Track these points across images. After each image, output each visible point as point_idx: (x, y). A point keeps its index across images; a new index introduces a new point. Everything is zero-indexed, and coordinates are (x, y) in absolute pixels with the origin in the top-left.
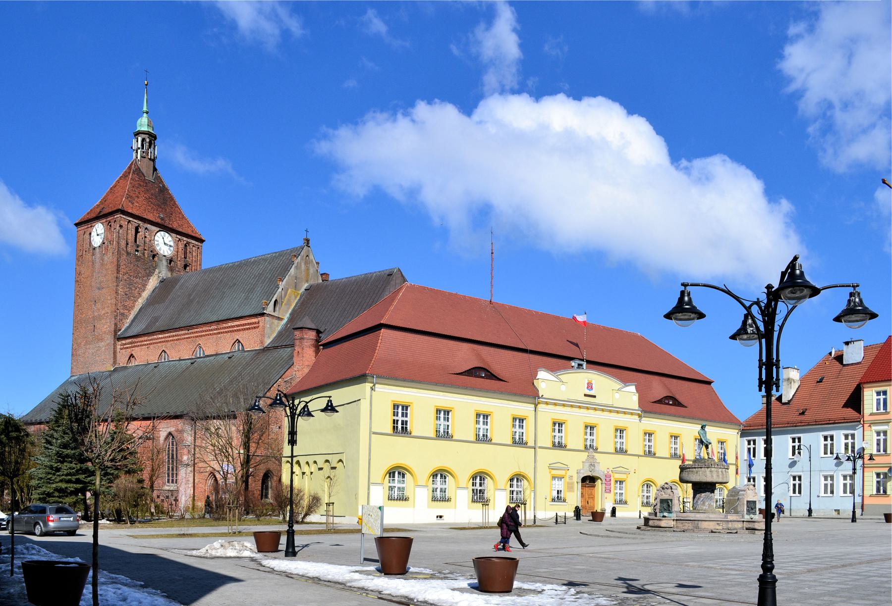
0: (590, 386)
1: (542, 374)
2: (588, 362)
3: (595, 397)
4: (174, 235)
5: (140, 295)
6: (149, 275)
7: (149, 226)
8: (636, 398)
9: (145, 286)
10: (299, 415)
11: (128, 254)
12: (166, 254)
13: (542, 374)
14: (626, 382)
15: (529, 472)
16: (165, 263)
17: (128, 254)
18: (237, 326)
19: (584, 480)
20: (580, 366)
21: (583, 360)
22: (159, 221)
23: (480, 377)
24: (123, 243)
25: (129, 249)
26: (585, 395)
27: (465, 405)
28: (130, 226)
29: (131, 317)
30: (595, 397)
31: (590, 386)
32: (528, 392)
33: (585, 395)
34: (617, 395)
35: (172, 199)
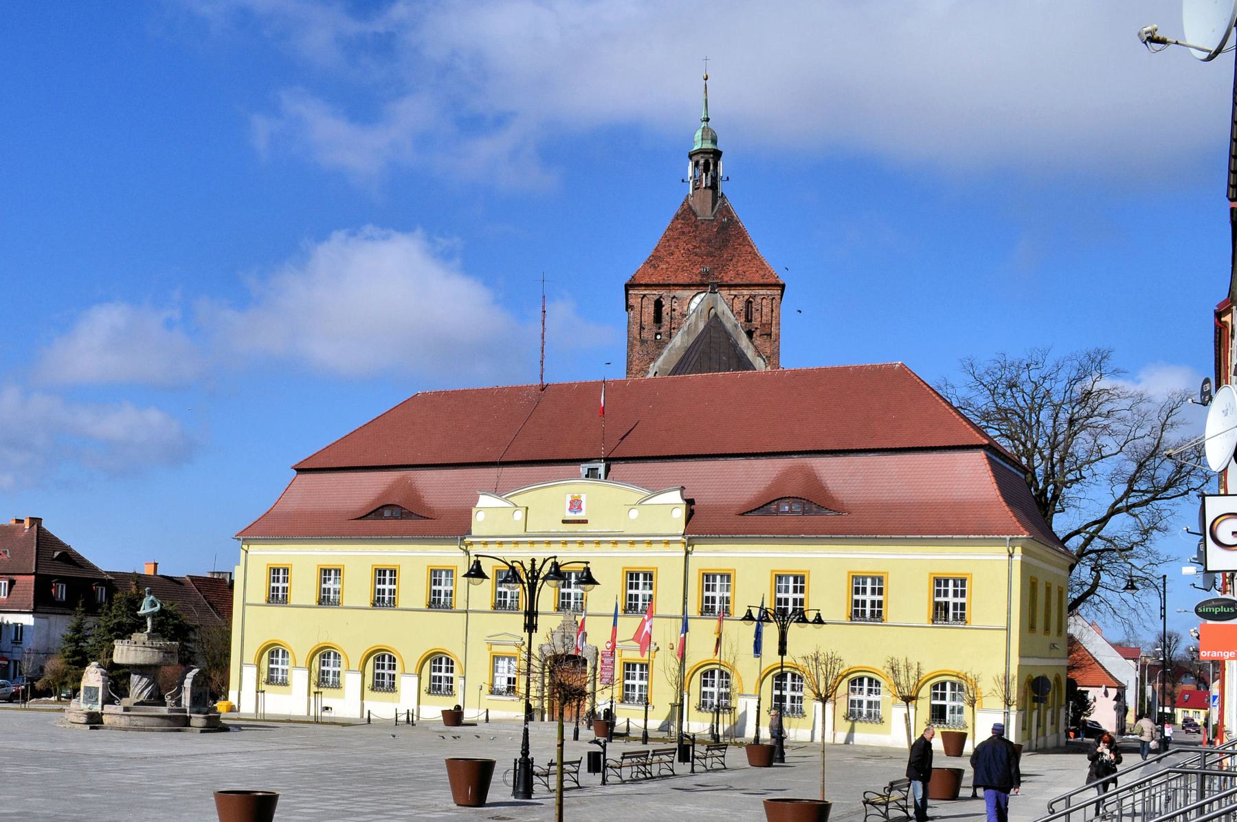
0: (576, 505)
1: (485, 501)
3: (585, 522)
7: (679, 293)
8: (680, 513)
10: (545, 578)
11: (643, 342)
13: (485, 501)
14: (657, 489)
15: (456, 653)
17: (643, 342)
22: (698, 279)
24: (636, 329)
25: (645, 335)
26: (564, 522)
27: (358, 559)
28: (645, 301)
30: (585, 522)
31: (576, 505)
32: (455, 527)
33: (564, 522)
34: (634, 514)
35: (741, 234)
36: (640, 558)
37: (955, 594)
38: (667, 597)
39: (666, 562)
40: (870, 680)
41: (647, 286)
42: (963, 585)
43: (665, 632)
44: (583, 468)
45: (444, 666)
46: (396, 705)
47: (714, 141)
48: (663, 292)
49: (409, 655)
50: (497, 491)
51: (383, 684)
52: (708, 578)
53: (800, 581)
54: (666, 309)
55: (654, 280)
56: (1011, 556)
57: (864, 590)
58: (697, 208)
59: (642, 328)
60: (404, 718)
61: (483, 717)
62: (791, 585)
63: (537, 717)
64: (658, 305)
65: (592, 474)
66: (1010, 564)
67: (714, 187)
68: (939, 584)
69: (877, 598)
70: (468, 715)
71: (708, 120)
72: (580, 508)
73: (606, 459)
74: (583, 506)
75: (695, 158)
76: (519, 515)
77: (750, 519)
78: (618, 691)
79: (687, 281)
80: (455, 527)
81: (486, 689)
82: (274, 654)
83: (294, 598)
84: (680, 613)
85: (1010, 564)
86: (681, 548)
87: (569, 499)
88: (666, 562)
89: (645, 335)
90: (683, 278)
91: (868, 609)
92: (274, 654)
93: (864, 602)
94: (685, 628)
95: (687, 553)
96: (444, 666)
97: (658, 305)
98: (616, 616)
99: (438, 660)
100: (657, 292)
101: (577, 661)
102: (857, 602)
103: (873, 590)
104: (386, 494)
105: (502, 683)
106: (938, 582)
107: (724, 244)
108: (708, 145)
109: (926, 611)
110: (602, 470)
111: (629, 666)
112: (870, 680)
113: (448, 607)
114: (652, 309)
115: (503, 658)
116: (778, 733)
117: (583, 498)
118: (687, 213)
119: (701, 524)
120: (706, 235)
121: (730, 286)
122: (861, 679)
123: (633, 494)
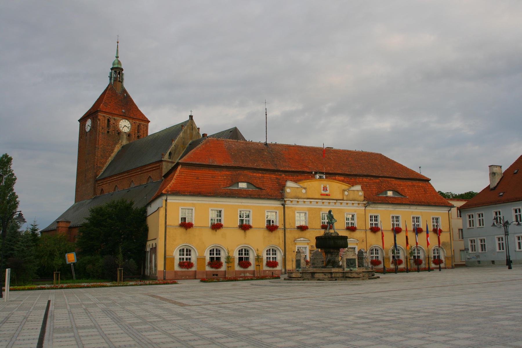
0: (325, 189)
1: (289, 184)
2: (327, 174)
3: (329, 195)
4: (131, 121)
5: (110, 156)
6: (116, 143)
7: (116, 118)
9: (113, 150)
12: (126, 131)
13: (289, 184)
16: (125, 136)
18: (150, 168)
20: (320, 177)
21: (323, 173)
26: (322, 195)
29: (104, 168)
30: (329, 195)
31: (325, 189)
50: (296, 181)
64: (109, 121)
72: (327, 190)
74: (328, 189)
87: (322, 186)
90: (117, 112)
97: (109, 121)
100: (107, 116)
110: (324, 177)
114: (106, 121)
117: (328, 186)
121: (133, 119)
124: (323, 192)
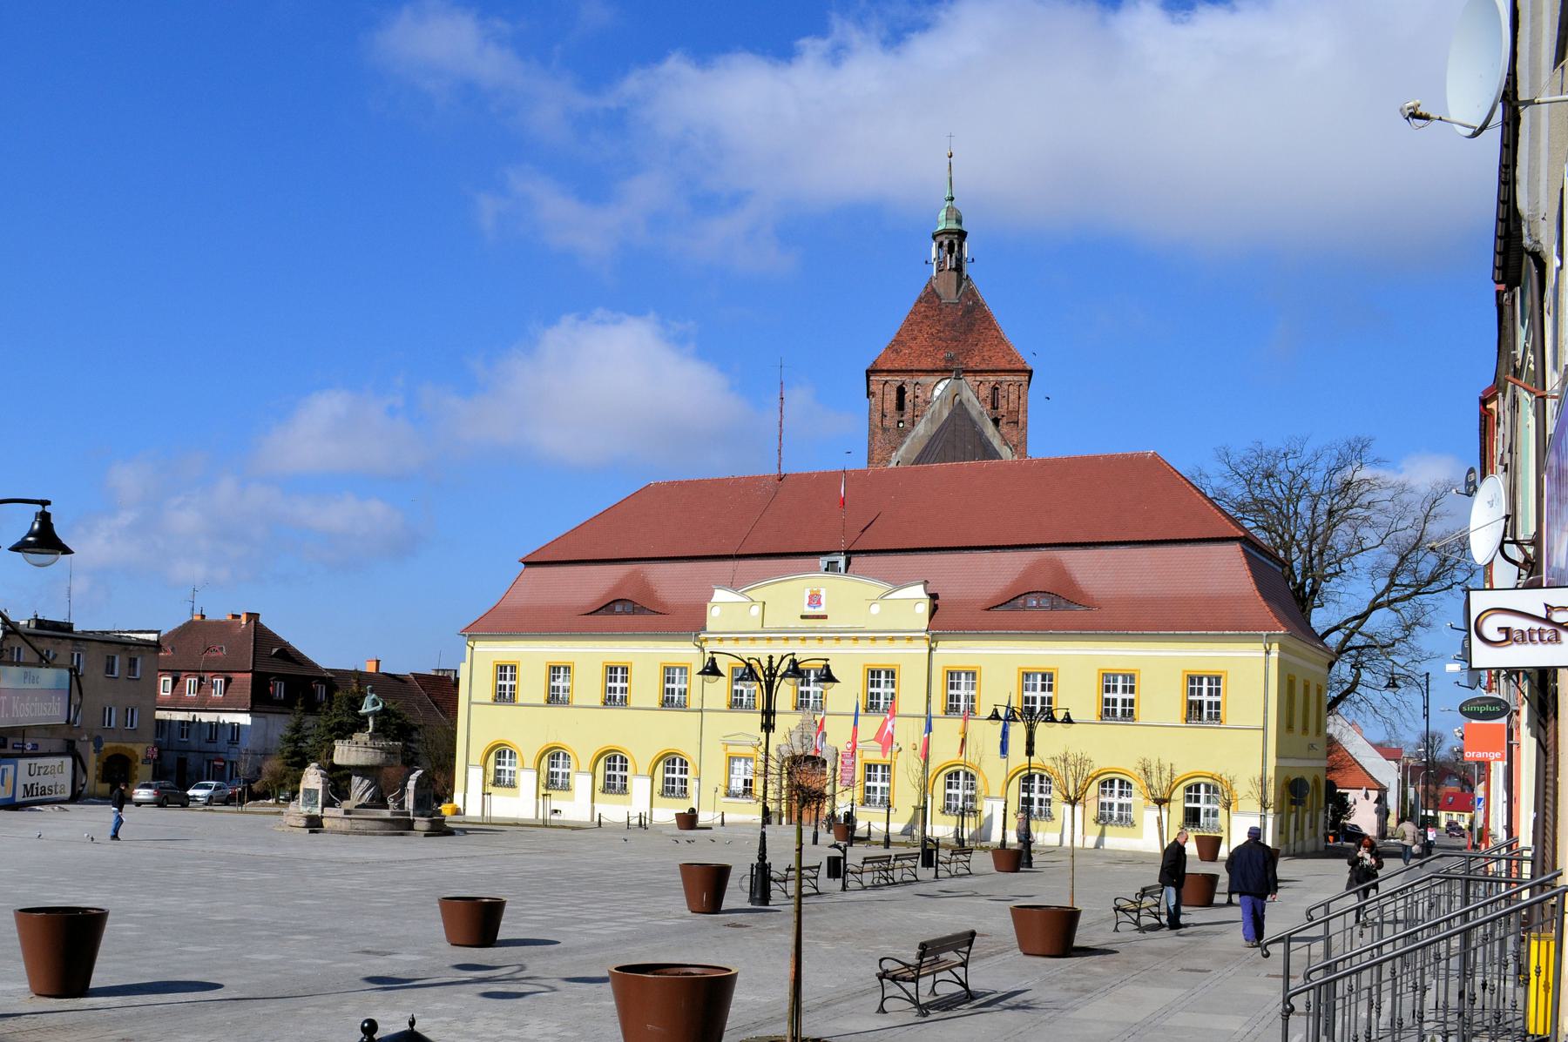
0: (815, 599)
1: (721, 595)
3: (825, 617)
7: (922, 379)
8: (923, 608)
10: (783, 676)
11: (885, 430)
13: (721, 595)
14: (899, 583)
15: (689, 752)
17: (885, 430)
19: (795, 760)
22: (941, 365)
23: (626, 612)
24: (877, 417)
27: (589, 657)
30: (825, 617)
31: (815, 599)
32: (690, 623)
34: (875, 609)
35: (987, 318)
36: (882, 654)
37: (1210, 692)
38: (910, 695)
39: (909, 658)
40: (1122, 782)
41: (889, 371)
42: (1218, 683)
43: (907, 732)
44: (823, 561)
45: (677, 767)
46: (628, 808)
47: (959, 221)
48: (906, 378)
49: (641, 757)
50: (733, 585)
51: (614, 785)
52: (953, 676)
53: (1048, 679)
54: (908, 396)
55: (897, 366)
56: (1268, 652)
57: (1115, 688)
58: (941, 291)
59: (884, 415)
60: (636, 821)
61: (719, 820)
62: (1039, 682)
63: (775, 820)
64: (901, 391)
65: (831, 567)
66: (1267, 662)
67: (959, 269)
68: (1193, 682)
69: (1128, 696)
70: (703, 818)
71: (952, 199)
72: (819, 603)
73: (846, 552)
74: (823, 601)
75: (939, 239)
76: (756, 610)
77: (997, 615)
78: (858, 794)
79: (931, 367)
80: (690, 623)
81: (722, 790)
82: (501, 754)
83: (521, 697)
84: (923, 712)
85: (1267, 662)
86: (925, 644)
87: (808, 593)
88: (909, 658)
89: (887, 422)
90: (927, 364)
91: (1119, 708)
92: (501, 754)
93: (1115, 701)
94: (929, 728)
95: (931, 649)
96: (677, 767)
97: (901, 391)
98: (857, 715)
99: (671, 760)
100: (896, 380)
101: (816, 761)
102: (1107, 701)
103: (1124, 689)
104: (616, 589)
105: (738, 785)
106: (1192, 680)
107: (970, 328)
108: (953, 226)
109: (1178, 710)
111: (870, 767)
112: (1122, 782)
113: (682, 706)
115: (740, 759)
116: (1026, 837)
117: (823, 593)
118: (930, 297)
119: (944, 618)
120: (950, 319)
121: (975, 372)
122: (1112, 781)
123: (875, 588)
124: (809, 611)
